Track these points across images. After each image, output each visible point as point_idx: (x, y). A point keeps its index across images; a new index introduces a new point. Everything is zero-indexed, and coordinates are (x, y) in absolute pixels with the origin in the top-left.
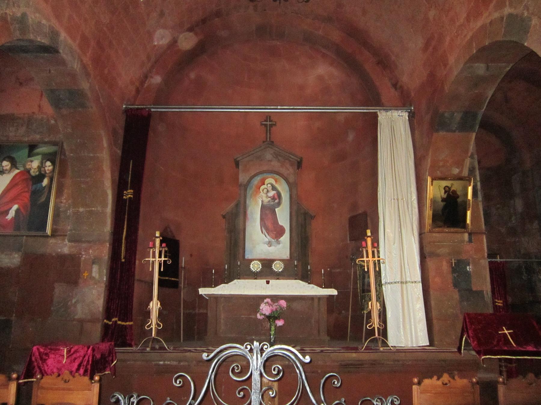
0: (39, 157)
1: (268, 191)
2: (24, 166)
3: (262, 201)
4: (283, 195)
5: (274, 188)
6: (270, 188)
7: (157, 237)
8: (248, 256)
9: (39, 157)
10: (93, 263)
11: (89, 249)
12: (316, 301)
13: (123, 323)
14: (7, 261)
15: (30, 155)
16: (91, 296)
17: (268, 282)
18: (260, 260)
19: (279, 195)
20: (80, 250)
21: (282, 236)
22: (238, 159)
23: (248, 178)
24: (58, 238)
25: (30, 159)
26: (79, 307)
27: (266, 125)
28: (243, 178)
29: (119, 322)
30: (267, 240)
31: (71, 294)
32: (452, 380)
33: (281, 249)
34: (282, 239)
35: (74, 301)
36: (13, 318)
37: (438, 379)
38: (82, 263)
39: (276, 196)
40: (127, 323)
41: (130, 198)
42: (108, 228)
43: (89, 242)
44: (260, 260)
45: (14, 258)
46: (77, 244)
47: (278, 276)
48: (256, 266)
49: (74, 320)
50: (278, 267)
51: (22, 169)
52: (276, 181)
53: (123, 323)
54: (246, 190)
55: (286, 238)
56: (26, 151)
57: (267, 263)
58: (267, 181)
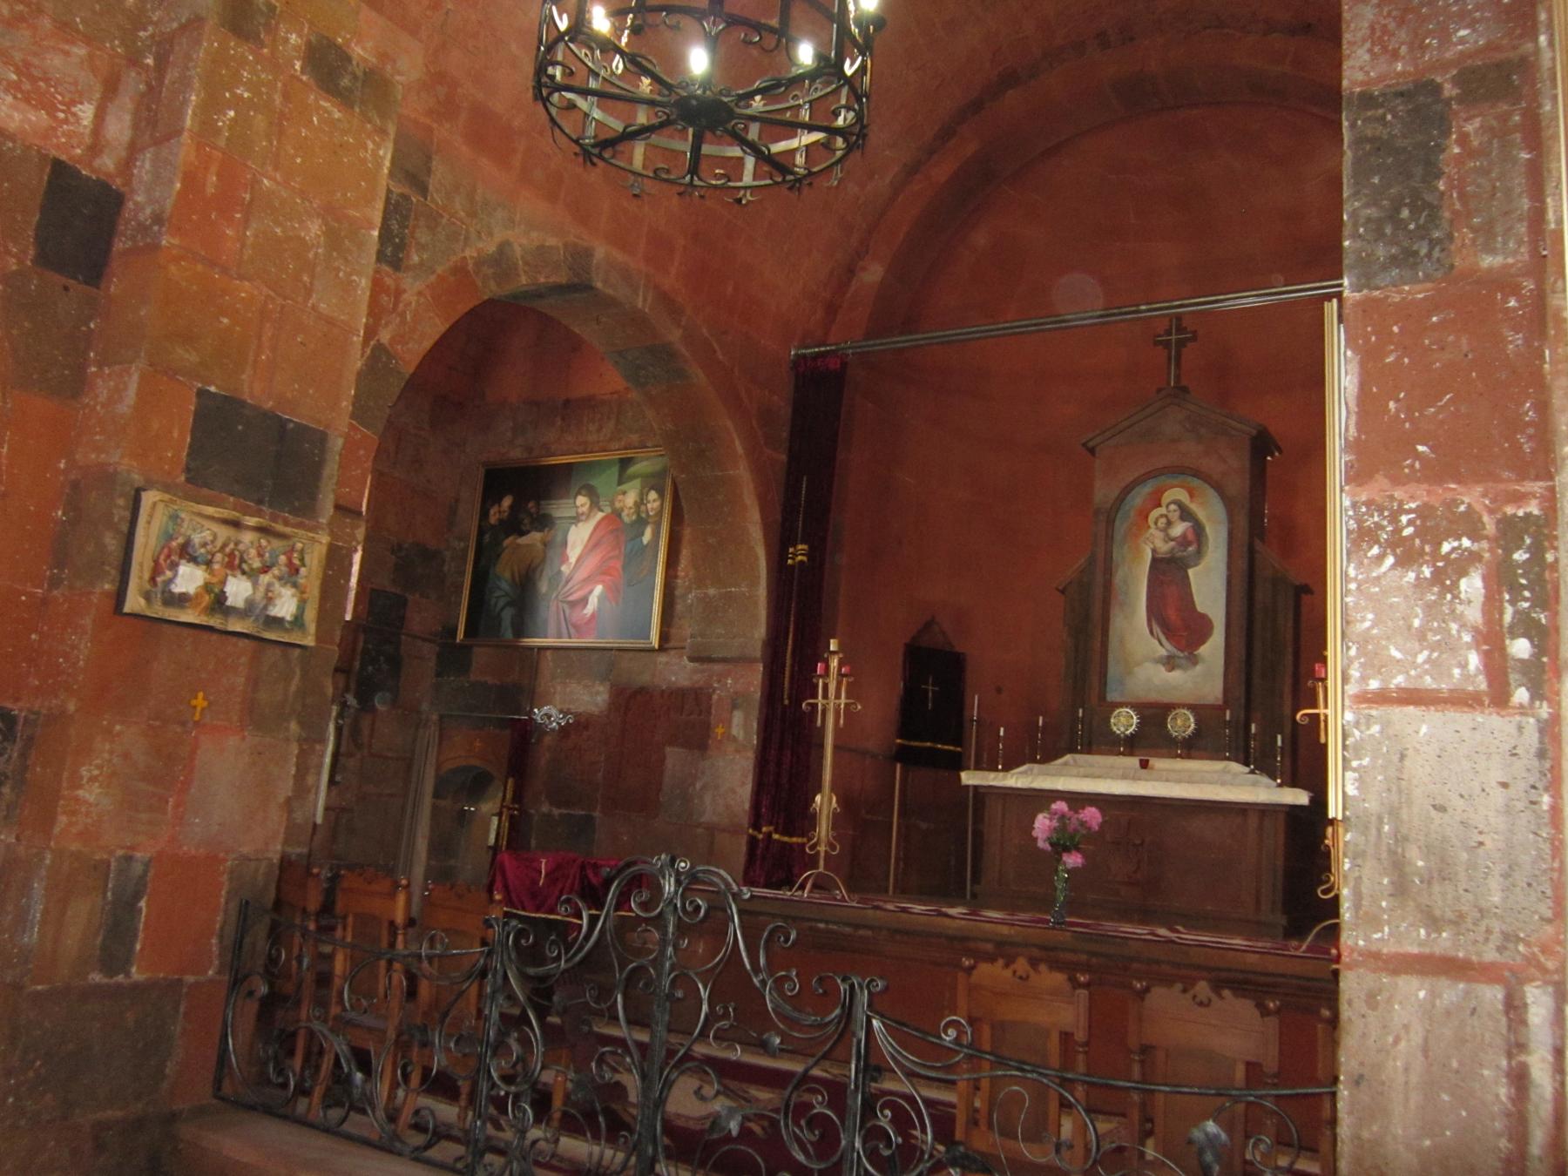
0: (637, 483)
1: (1169, 523)
2: (612, 504)
3: (1154, 551)
4: (1208, 529)
5: (1186, 514)
6: (1175, 516)
7: (834, 653)
8: (1112, 696)
9: (637, 483)
10: (734, 707)
12: (1253, 821)
13: (786, 839)
14: (586, 698)
15: (620, 483)
16: (729, 779)
17: (1144, 765)
18: (1192, 708)
19: (1198, 529)
21: (1203, 642)
22: (1091, 444)
23: (1116, 493)
25: (623, 487)
26: (708, 799)
27: (1167, 344)
28: (1103, 492)
29: (776, 836)
30: (1162, 652)
32: (1032, 973)
33: (1204, 676)
34: (1203, 650)
35: (698, 786)
36: (597, 814)
37: (1007, 965)
39: (1191, 536)
40: (794, 840)
41: (801, 562)
42: (761, 632)
43: (724, 660)
44: (1192, 708)
45: (598, 693)
46: (705, 666)
47: (1190, 748)
48: (1125, 722)
49: (699, 825)
50: (1182, 724)
51: (608, 510)
52: (1192, 496)
53: (786, 839)
54: (1110, 522)
55: (1213, 649)
56: (615, 470)
57: (1154, 715)
58: (1168, 496)
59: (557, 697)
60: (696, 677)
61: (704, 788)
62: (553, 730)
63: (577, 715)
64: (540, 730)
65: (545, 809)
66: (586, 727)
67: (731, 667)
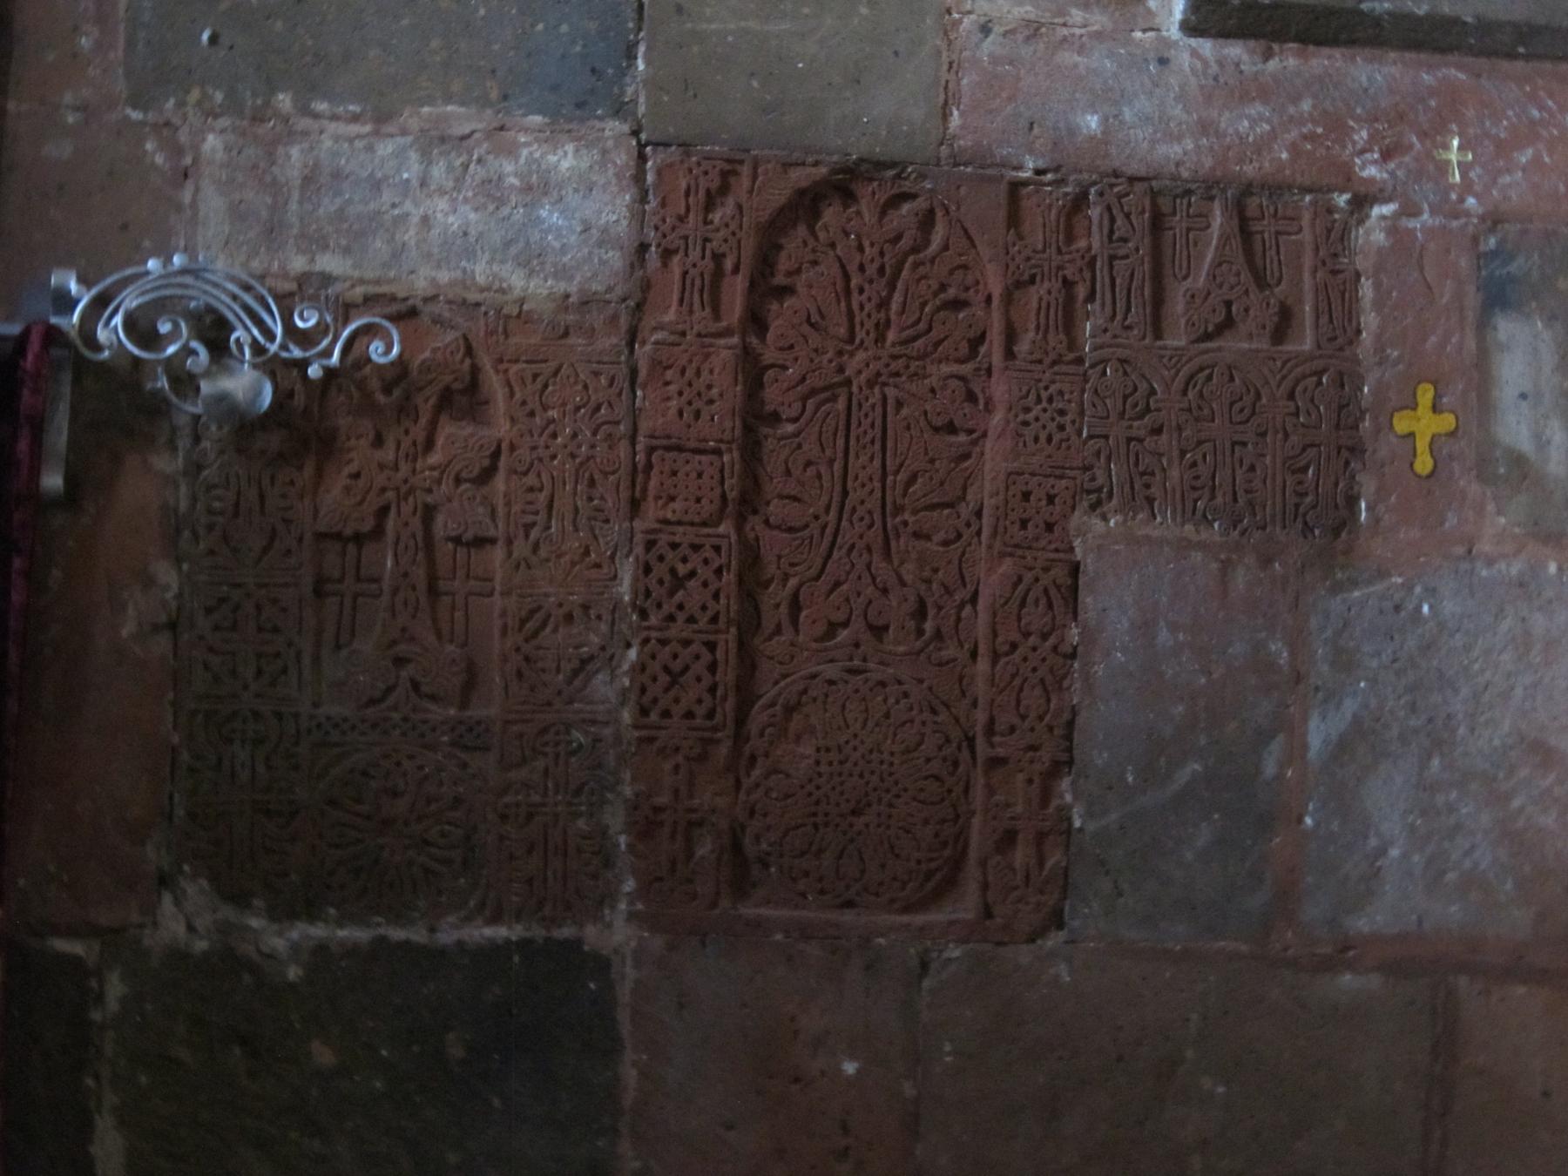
10: (1498, 297)
11: (1435, 134)
14: (453, 216)
20: (1337, 127)
26: (1387, 801)
31: (1278, 649)
35: (1319, 733)
36: (616, 932)
38: (1367, 289)
45: (539, 187)
46: (1287, 61)
49: (1345, 954)
61: (1358, 743)
64: (125, 406)
65: (183, 920)
66: (464, 397)
67: (1455, 73)
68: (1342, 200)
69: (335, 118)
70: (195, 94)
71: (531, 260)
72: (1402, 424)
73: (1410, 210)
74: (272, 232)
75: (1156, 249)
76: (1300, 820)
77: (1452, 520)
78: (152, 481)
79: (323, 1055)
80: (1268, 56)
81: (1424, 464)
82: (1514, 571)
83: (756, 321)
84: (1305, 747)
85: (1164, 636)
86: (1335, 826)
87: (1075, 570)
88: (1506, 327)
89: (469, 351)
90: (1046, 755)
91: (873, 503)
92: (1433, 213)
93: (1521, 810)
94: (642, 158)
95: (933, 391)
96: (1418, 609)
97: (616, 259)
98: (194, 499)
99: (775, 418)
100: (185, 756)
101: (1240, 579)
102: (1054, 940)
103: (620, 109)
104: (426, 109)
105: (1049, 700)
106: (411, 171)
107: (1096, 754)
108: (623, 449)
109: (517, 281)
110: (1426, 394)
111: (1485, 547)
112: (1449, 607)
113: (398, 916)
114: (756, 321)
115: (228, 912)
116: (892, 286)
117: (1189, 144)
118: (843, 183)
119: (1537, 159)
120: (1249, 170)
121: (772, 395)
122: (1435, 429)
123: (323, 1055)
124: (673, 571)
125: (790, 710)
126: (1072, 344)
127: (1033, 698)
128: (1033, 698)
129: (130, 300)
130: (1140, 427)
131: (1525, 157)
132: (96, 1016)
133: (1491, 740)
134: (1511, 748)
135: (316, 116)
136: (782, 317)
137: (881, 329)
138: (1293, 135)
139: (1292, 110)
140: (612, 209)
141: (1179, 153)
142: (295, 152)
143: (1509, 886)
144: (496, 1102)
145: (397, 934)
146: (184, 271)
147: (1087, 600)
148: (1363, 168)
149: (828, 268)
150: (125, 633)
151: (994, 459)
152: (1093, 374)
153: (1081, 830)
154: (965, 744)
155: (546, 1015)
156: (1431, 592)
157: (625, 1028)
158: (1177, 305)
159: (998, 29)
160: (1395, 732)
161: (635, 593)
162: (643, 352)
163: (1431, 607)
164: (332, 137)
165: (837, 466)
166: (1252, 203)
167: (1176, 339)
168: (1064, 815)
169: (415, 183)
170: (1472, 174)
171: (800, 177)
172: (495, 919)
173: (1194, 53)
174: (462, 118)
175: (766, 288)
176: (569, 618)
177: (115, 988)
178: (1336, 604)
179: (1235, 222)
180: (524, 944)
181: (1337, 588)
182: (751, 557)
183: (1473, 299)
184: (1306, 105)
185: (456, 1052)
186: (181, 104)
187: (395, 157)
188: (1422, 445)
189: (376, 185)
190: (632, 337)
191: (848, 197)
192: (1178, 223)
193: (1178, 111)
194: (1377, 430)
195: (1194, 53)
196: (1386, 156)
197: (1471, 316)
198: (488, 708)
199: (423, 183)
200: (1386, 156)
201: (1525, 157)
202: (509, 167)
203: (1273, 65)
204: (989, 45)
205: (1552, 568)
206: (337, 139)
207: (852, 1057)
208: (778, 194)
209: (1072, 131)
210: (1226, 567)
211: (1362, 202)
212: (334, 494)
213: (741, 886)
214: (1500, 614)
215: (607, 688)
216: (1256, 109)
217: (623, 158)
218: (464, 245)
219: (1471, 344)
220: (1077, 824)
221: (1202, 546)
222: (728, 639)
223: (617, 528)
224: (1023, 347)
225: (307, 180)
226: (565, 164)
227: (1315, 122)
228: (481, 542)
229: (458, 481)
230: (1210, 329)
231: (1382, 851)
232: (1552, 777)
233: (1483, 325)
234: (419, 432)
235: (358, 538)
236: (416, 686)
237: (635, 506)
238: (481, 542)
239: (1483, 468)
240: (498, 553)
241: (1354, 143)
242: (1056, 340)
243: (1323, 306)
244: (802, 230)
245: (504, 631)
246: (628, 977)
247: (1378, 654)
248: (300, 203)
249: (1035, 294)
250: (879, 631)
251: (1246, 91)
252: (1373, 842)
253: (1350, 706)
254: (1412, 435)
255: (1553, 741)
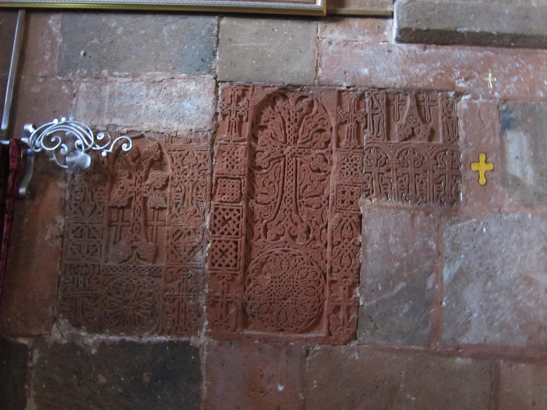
11: (483, 72)
14: (156, 105)
20: (449, 70)
24: (356, 23)
26: (472, 296)
31: (432, 244)
35: (447, 273)
36: (201, 339)
38: (461, 123)
45: (183, 96)
46: (432, 50)
49: (458, 350)
59: (81, 104)
60: (419, 70)
62: (79, 168)
63: (139, 137)
65: (59, 333)
66: (158, 162)
67: (489, 52)
68: (451, 94)
69: (120, 77)
70: (78, 71)
71: (181, 118)
72: (474, 167)
73: (475, 97)
74: (99, 112)
75: (388, 113)
76: (441, 303)
77: (493, 200)
78: (57, 191)
79: (102, 380)
80: (425, 49)
81: (482, 181)
82: (516, 217)
83: (254, 137)
84: (442, 278)
85: (391, 239)
86: (454, 305)
87: (361, 217)
88: (510, 135)
89: (160, 147)
90: (350, 280)
91: (292, 195)
92: (483, 97)
93: (521, 300)
94: (217, 86)
95: (313, 158)
96: (482, 229)
97: (208, 118)
98: (71, 196)
99: (260, 168)
100: (62, 279)
101: (418, 219)
102: (353, 344)
103: (210, 71)
104: (149, 73)
105: (351, 261)
106: (144, 92)
107: (367, 280)
108: (208, 178)
109: (175, 126)
110: (482, 158)
111: (505, 209)
112: (493, 229)
113: (129, 334)
114: (254, 137)
115: (74, 331)
116: (299, 126)
117: (399, 78)
118: (283, 92)
119: (519, 79)
120: (420, 85)
121: (259, 160)
122: (486, 169)
123: (102, 380)
124: (224, 218)
125: (263, 264)
126: (359, 142)
127: (346, 261)
128: (346, 261)
129: (46, 133)
130: (383, 169)
131: (515, 79)
132: (30, 364)
133: (509, 276)
134: (517, 278)
135: (115, 76)
136: (262, 136)
137: (296, 139)
138: (434, 73)
139: (433, 65)
140: (206, 102)
141: (395, 80)
142: (108, 87)
143: (517, 327)
144: (159, 397)
145: (128, 339)
146: (65, 124)
147: (364, 227)
148: (459, 83)
149: (278, 120)
150: (46, 239)
151: (333, 181)
152: (367, 152)
153: (362, 306)
154: (322, 276)
155: (176, 366)
156: (486, 224)
157: (204, 373)
158: (395, 128)
159: (334, 43)
160: (474, 272)
161: (211, 225)
162: (215, 147)
163: (486, 229)
164: (120, 82)
165: (281, 183)
166: (421, 97)
167: (395, 140)
168: (357, 301)
169: (144, 96)
170: (496, 85)
171: (268, 91)
172: (161, 334)
173: (400, 48)
174: (160, 76)
175: (257, 126)
176: (189, 233)
177: (36, 355)
178: (453, 228)
179: (415, 102)
180: (171, 342)
181: (453, 223)
182: (251, 213)
183: (498, 126)
184: (439, 64)
185: (146, 379)
186: (74, 74)
187: (138, 87)
188: (482, 174)
189: (132, 97)
190: (213, 142)
191: (285, 97)
192: (395, 103)
193: (395, 67)
194: (466, 169)
195: (400, 48)
196: (466, 80)
197: (497, 131)
198: (162, 264)
199: (147, 96)
200: (466, 80)
201: (515, 79)
202: (174, 90)
203: (427, 52)
204: (331, 48)
205: (530, 216)
206: (120, 83)
207: (281, 385)
208: (260, 96)
209: (359, 74)
210: (413, 216)
211: (459, 95)
212: (116, 194)
213: (245, 325)
214: (511, 232)
215: (200, 256)
216: (422, 65)
217: (211, 85)
218: (160, 114)
219: (498, 140)
220: (361, 303)
221: (405, 209)
222: (242, 240)
223: (205, 205)
224: (343, 143)
225: (111, 96)
226: (192, 88)
227: (442, 69)
228: (161, 209)
229: (155, 189)
230: (407, 137)
231: (471, 314)
232: (532, 289)
233: (502, 133)
234: (143, 174)
235: (122, 208)
236: (138, 255)
237: (212, 196)
238: (161, 209)
239: (504, 182)
240: (167, 212)
241: (455, 76)
242: (354, 141)
243: (446, 129)
244: (270, 108)
245: (168, 237)
246: (205, 355)
247: (468, 246)
248: (109, 103)
249: (346, 126)
250: (294, 238)
251: (417, 60)
252: (468, 311)
253: (458, 264)
254: (478, 171)
255: (532, 276)
